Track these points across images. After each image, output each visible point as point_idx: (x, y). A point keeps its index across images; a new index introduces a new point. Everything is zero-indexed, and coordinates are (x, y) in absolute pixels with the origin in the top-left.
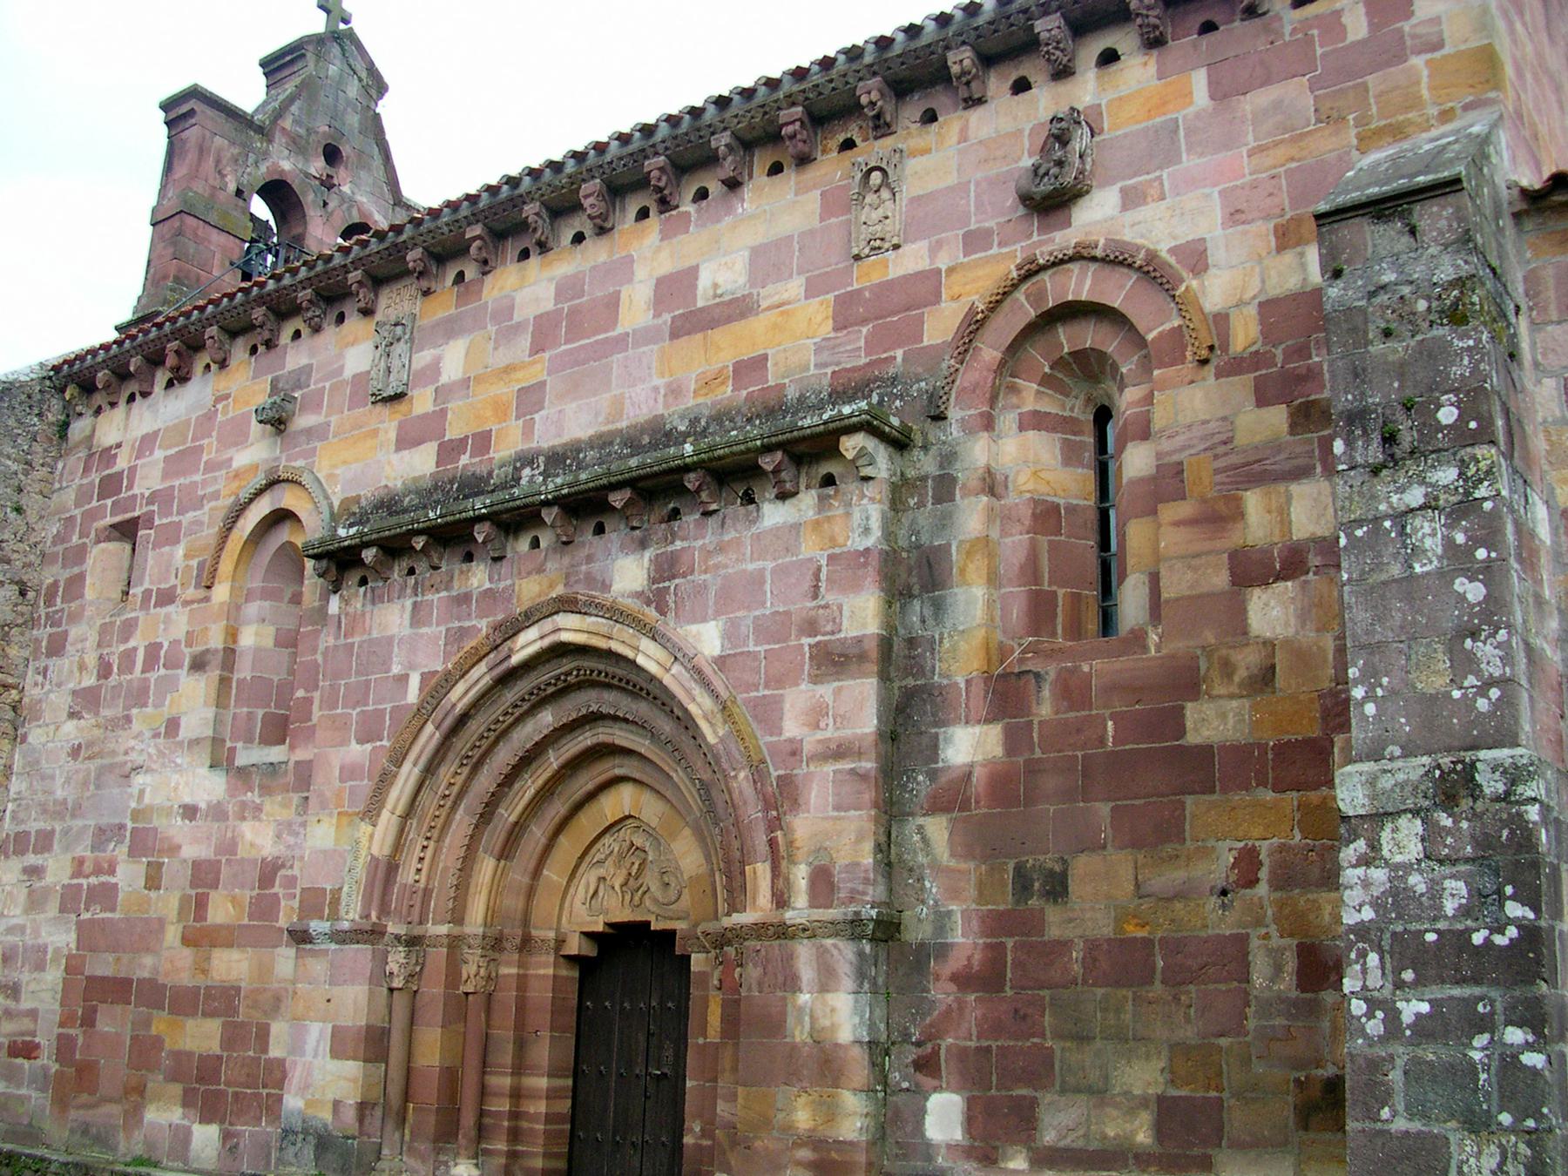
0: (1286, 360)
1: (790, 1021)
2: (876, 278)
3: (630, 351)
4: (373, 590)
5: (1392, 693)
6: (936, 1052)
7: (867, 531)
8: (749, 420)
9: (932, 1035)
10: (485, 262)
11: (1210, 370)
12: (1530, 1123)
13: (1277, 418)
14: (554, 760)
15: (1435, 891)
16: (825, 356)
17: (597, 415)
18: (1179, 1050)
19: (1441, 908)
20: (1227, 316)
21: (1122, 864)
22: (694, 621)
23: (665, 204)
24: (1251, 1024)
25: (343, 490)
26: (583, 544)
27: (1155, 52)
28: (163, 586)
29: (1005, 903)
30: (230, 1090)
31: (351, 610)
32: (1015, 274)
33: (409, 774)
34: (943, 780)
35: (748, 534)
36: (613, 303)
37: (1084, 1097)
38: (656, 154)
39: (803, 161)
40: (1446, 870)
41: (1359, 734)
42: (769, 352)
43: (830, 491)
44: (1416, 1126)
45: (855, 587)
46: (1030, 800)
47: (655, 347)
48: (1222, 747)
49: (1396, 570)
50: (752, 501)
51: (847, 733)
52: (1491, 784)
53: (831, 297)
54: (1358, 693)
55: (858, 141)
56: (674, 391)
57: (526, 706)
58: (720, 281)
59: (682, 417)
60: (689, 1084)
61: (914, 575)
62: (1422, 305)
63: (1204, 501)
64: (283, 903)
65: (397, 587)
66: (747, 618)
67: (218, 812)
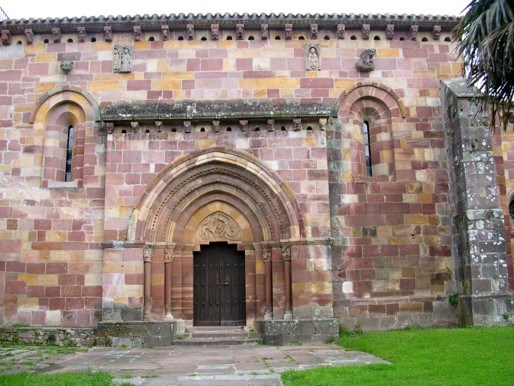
0: (422, 121)
1: (308, 266)
2: (313, 77)
3: (228, 78)
4: (129, 135)
5: (475, 197)
6: (344, 272)
7: (323, 143)
8: (274, 106)
9: (343, 268)
10: (166, 37)
11: (405, 119)
12: (505, 277)
13: (421, 134)
14: (198, 194)
15: (487, 235)
16: (298, 94)
17: (217, 94)
18: (404, 269)
19: (487, 238)
20: (409, 108)
21: (389, 229)
22: (268, 160)
23: (240, 38)
24: (420, 263)
25: (102, 99)
26: (223, 133)
27: (389, 41)
28: (4, 119)
29: (361, 237)
30: (65, 298)
31: (119, 140)
32: (356, 86)
33: (152, 196)
34: (342, 207)
35: (284, 139)
36: (220, 62)
37: (382, 281)
38: (242, 23)
39: (288, 39)
40: (488, 231)
41: (469, 204)
42: (280, 89)
43: (311, 131)
44: (485, 278)
45: (320, 157)
46: (366, 213)
47: (238, 79)
48: (411, 204)
49: (475, 173)
50: (285, 130)
51: (320, 194)
52: (496, 215)
53: (299, 78)
54: (469, 196)
55: (305, 38)
56: (246, 93)
58: (261, 65)
59: (250, 101)
60: (246, 286)
61: (334, 156)
62: (479, 121)
63: (405, 149)
64: (86, 235)
65: (141, 136)
66: (287, 162)
67: (47, 203)
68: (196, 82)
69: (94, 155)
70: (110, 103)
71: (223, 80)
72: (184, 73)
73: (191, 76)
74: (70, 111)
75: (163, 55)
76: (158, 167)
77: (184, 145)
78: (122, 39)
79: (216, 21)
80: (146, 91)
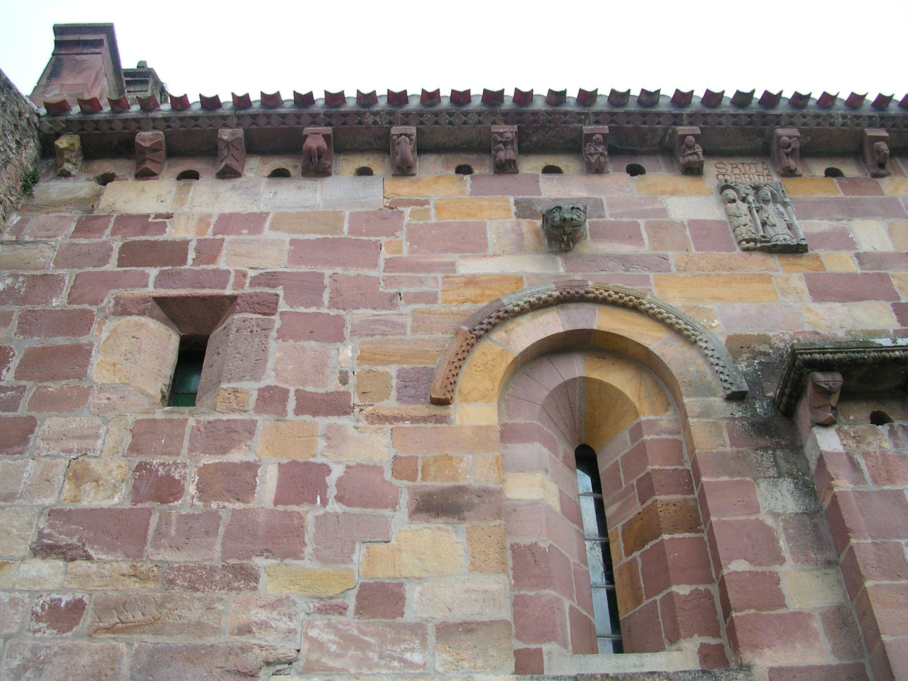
10: (882, 166)
28: (310, 389)
69: (762, 523)
70: (765, 340)
74: (595, 375)
75: (890, 210)
78: (736, 171)
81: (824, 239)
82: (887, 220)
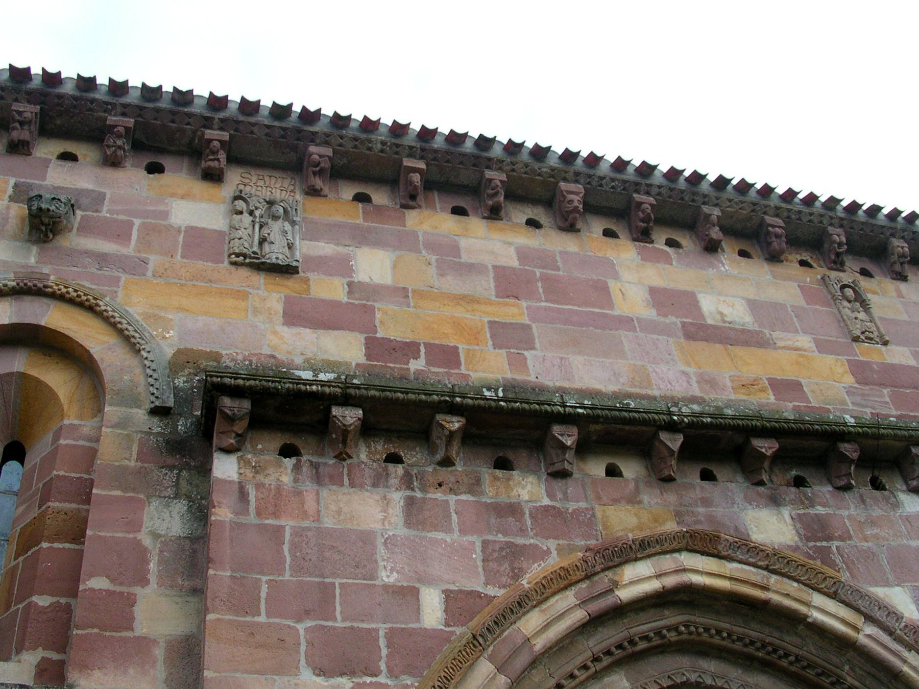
4: (315, 466)
10: (413, 197)
31: (269, 481)
38: (648, 193)
57: (607, 661)
68: (535, 330)
69: (138, 543)
70: (216, 357)
71: (624, 336)
72: (488, 302)
73: (515, 312)
74: (34, 372)
75: (407, 243)
76: (458, 604)
77: (550, 519)
78: (261, 183)
79: (577, 174)
80: (361, 338)
81: (322, 264)
82: (398, 253)
